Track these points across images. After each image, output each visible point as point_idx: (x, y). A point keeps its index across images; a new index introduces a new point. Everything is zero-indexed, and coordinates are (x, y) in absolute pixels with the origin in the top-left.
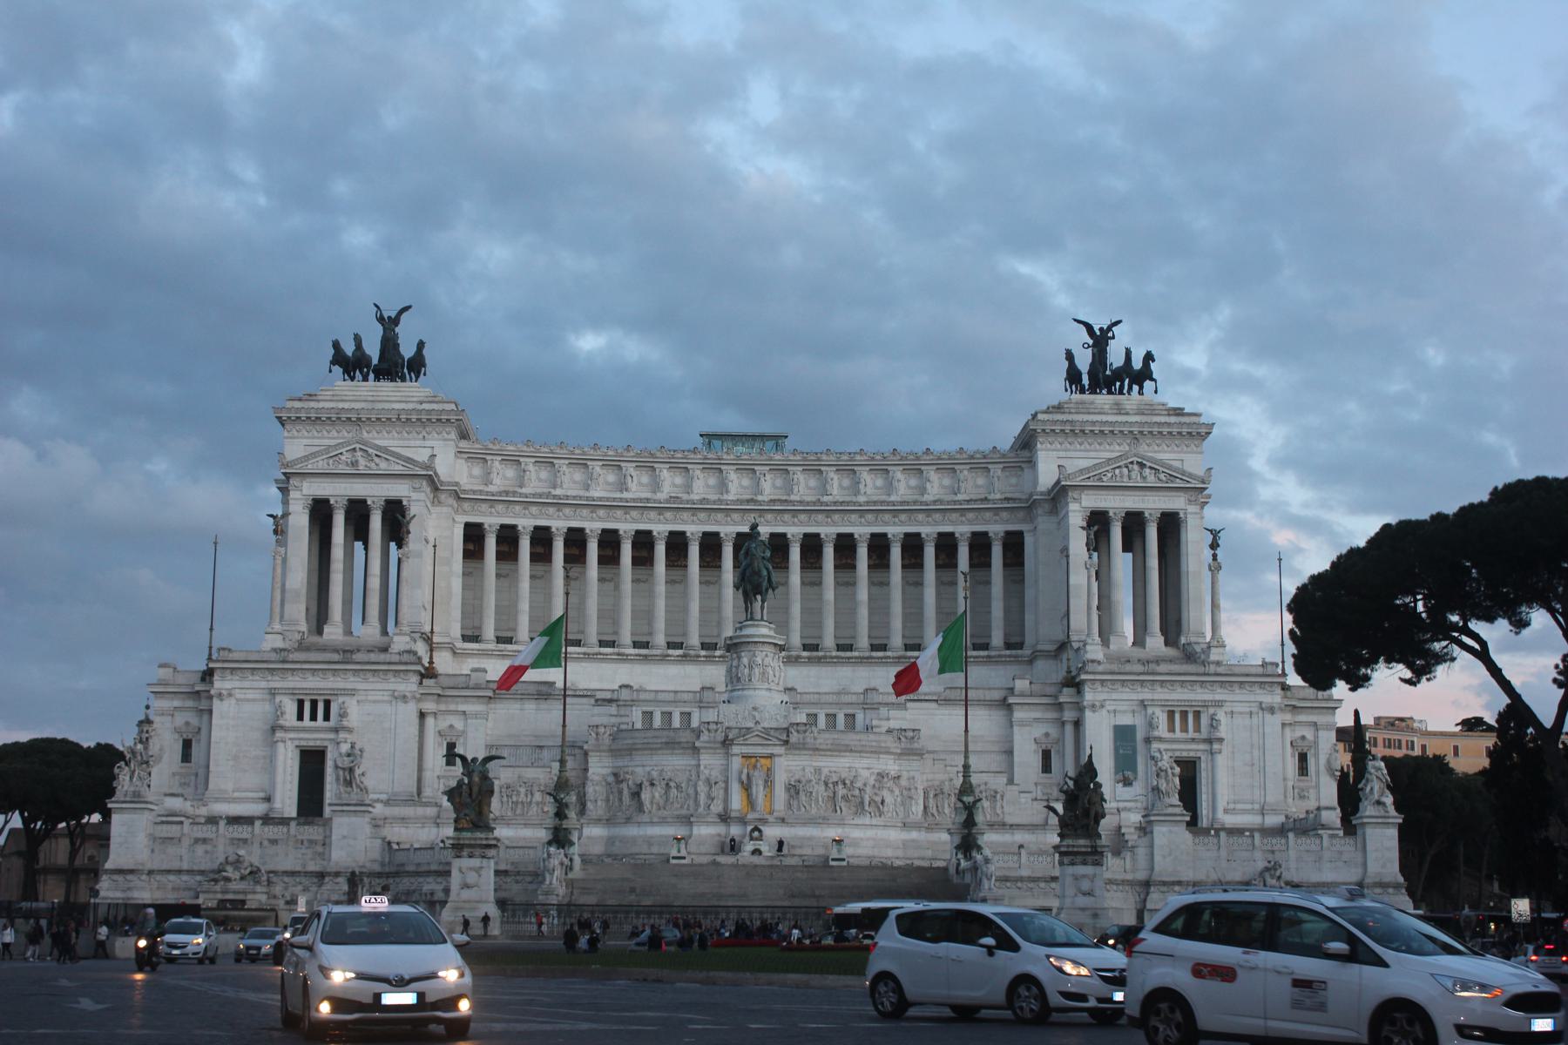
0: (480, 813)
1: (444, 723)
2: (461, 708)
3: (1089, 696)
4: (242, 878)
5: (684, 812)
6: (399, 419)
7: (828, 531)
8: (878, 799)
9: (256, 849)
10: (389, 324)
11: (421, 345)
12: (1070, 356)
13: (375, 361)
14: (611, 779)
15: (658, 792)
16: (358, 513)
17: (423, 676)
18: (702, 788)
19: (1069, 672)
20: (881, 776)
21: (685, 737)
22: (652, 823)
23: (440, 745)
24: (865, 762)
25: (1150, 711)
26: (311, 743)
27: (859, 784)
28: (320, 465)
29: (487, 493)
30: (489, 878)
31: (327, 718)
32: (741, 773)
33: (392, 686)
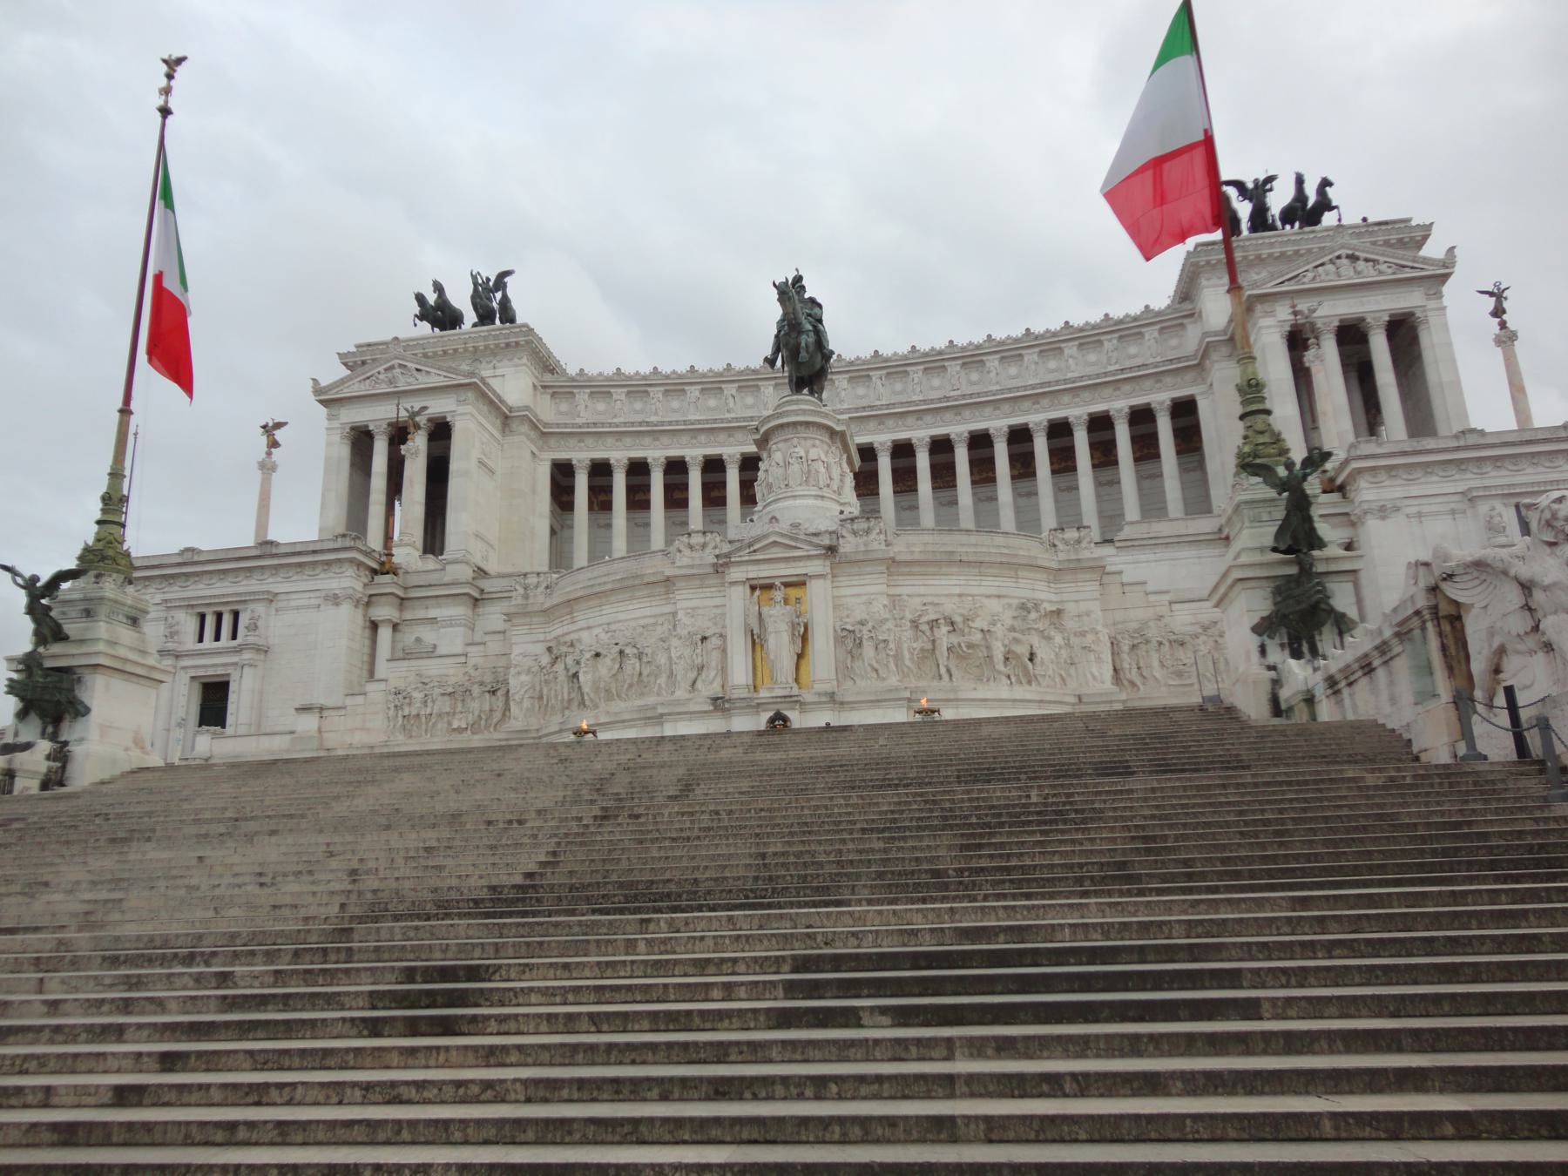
1: (408, 637)
2: (432, 613)
3: (1367, 493)
5: (651, 700)
6: (466, 350)
7: (958, 429)
8: (1022, 650)
11: (505, 285)
13: (470, 317)
14: (546, 660)
15: (605, 668)
16: (399, 434)
17: (374, 572)
21: (654, 566)
24: (989, 585)
25: (1483, 508)
26: (211, 672)
27: (978, 624)
28: (355, 389)
29: (573, 425)
32: (746, 616)
33: (311, 585)
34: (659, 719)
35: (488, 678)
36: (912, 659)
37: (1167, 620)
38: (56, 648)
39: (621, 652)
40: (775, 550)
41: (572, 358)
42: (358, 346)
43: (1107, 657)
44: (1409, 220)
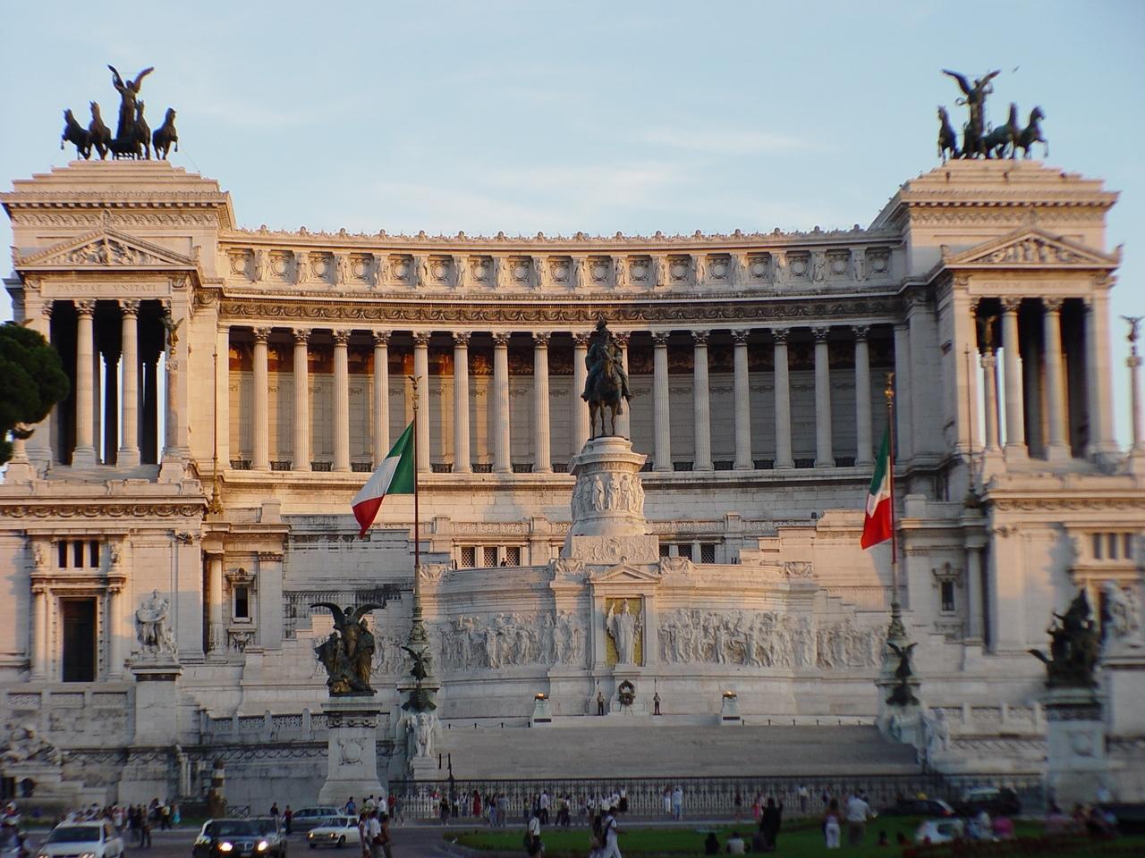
0: (359, 673)
3: (999, 518)
4: (31, 758)
6: (150, 205)
9: (46, 725)
10: (128, 91)
11: (170, 115)
12: (943, 116)
14: (447, 629)
16: (108, 315)
17: (206, 511)
18: (559, 636)
19: (972, 491)
20: (768, 617)
22: (502, 681)
23: (228, 590)
25: (1072, 535)
27: (744, 629)
28: (62, 263)
30: (370, 755)
31: (95, 563)
34: (547, 680)
35: (391, 633)
36: (703, 650)
37: (852, 623)
38: (424, 681)
39: (518, 633)
40: (624, 577)
41: (252, 214)
42: (16, 183)
43: (815, 648)
44: (1100, 182)
